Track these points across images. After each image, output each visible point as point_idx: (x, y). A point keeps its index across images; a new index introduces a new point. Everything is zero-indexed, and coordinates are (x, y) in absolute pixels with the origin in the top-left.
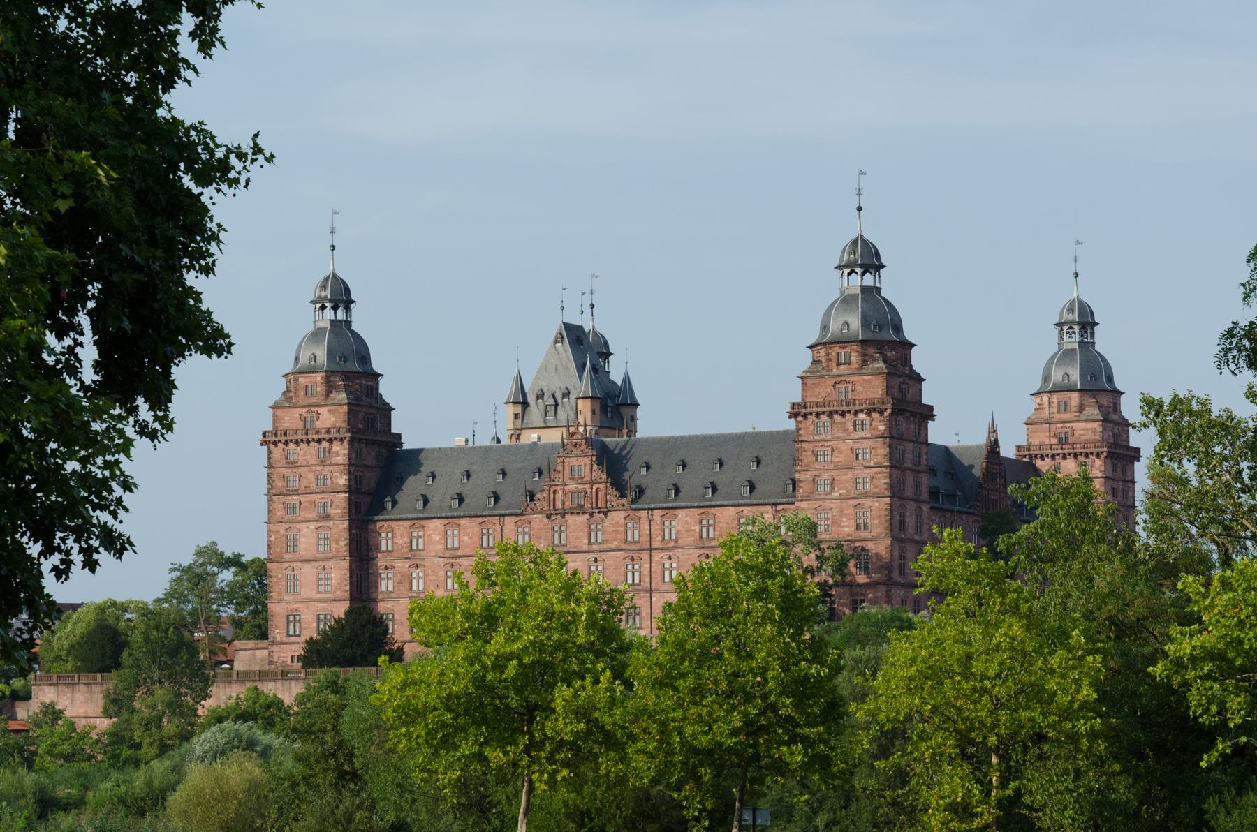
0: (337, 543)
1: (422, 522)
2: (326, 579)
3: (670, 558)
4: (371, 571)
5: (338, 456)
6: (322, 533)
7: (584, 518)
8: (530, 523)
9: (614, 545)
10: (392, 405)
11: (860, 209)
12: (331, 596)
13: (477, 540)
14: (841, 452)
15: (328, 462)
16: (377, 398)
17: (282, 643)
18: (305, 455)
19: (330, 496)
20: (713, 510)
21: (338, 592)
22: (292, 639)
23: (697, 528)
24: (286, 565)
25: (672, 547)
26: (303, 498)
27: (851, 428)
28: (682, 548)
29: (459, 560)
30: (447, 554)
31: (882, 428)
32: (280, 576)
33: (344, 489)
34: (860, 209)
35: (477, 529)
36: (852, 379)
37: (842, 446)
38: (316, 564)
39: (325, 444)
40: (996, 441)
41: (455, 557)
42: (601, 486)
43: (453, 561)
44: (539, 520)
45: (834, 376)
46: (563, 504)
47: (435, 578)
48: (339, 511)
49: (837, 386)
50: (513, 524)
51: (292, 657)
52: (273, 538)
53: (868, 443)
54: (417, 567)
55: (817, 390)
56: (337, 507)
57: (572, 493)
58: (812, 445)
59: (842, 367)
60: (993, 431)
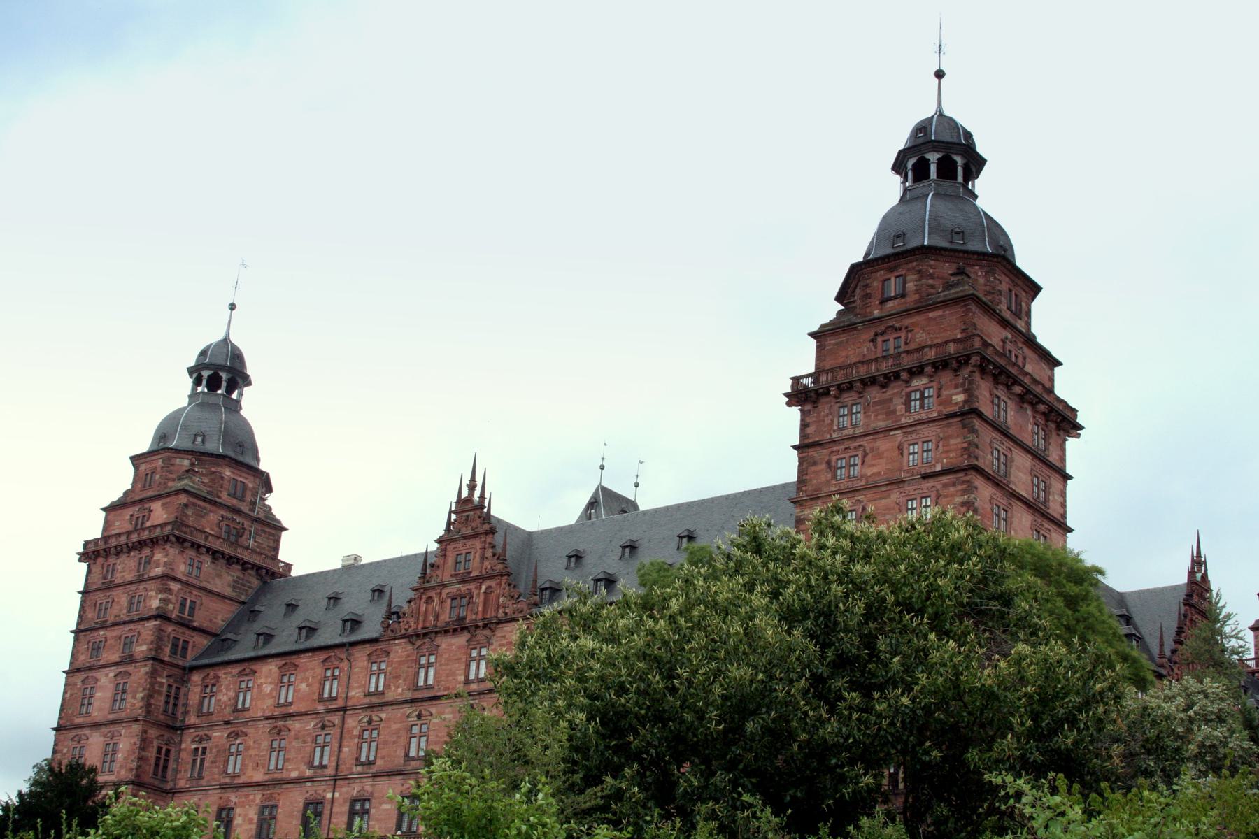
0: (134, 697)
2: (114, 753)
4: (183, 746)
8: (388, 653)
10: (285, 524)
11: (940, 74)
13: (316, 686)
14: (879, 456)
15: (146, 576)
16: (253, 503)
21: (123, 772)
24: (73, 733)
27: (900, 408)
29: (289, 722)
31: (960, 398)
32: (65, 751)
33: (155, 613)
34: (940, 74)
35: (319, 670)
37: (884, 445)
38: (105, 730)
39: (147, 551)
40: (1205, 577)
41: (285, 717)
42: (492, 583)
43: (281, 723)
48: (144, 648)
49: (880, 339)
50: (365, 658)
52: (68, 695)
54: (237, 735)
55: (844, 354)
58: (826, 451)
59: (890, 304)
60: (1198, 562)
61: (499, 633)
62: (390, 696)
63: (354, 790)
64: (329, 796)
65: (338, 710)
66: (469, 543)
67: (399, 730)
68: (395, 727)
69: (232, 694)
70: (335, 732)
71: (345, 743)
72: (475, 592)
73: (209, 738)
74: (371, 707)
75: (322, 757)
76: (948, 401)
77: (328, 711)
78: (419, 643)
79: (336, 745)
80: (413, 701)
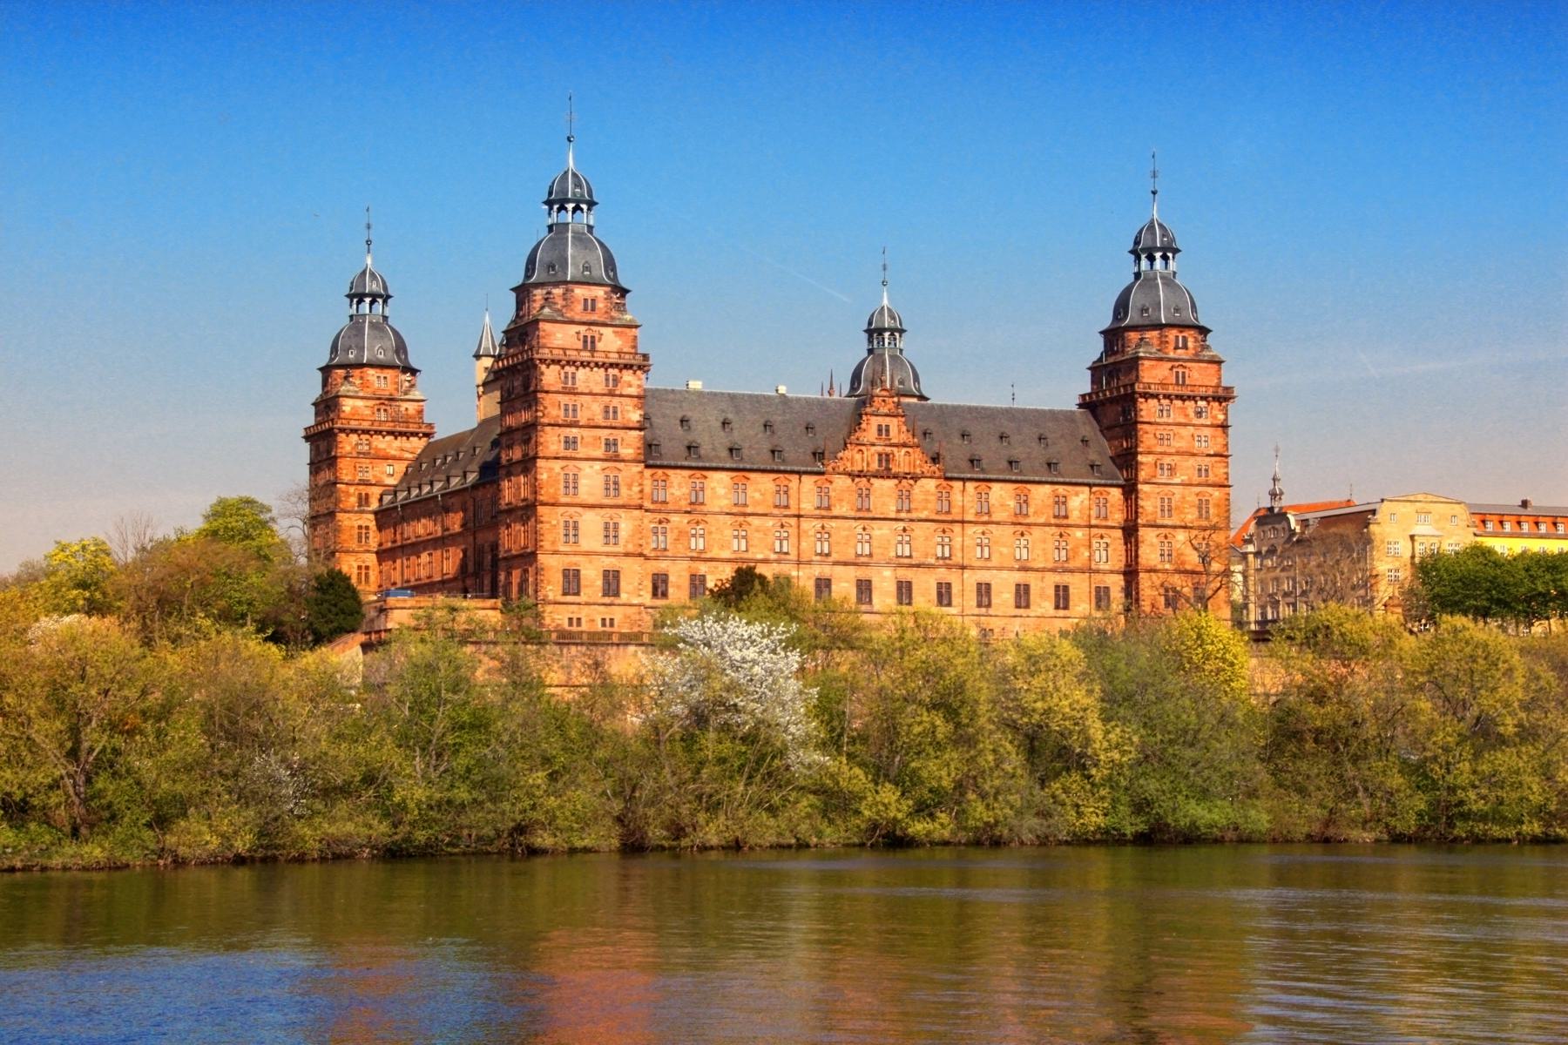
1: (705, 473)
3: (983, 533)
5: (630, 386)
6: (607, 472)
7: (892, 483)
8: (831, 482)
9: (923, 515)
11: (1154, 193)
12: (619, 549)
15: (617, 392)
17: (556, 603)
18: (587, 381)
19: (619, 434)
20: (1029, 486)
22: (569, 599)
23: (1012, 503)
24: (561, 510)
25: (985, 518)
26: (586, 433)
28: (998, 523)
29: (749, 519)
30: (735, 510)
31: (1221, 417)
32: (554, 522)
33: (637, 425)
34: (1154, 193)
36: (1188, 364)
39: (612, 371)
41: (745, 515)
42: (910, 450)
43: (741, 519)
44: (841, 482)
45: (1170, 360)
46: (868, 464)
47: (719, 536)
48: (631, 451)
51: (570, 619)
53: (1207, 432)
54: (698, 523)
56: (629, 446)
57: (880, 455)
58: (1153, 427)
61: (919, 483)
62: (835, 512)
63: (817, 571)
64: (794, 573)
65: (795, 516)
66: (888, 419)
67: (847, 537)
68: (846, 533)
69: (685, 490)
70: (793, 531)
71: (802, 539)
72: (897, 454)
73: (668, 521)
74: (823, 517)
75: (781, 546)
76: (1215, 417)
77: (786, 516)
78: (857, 480)
79: (796, 540)
80: (860, 518)
